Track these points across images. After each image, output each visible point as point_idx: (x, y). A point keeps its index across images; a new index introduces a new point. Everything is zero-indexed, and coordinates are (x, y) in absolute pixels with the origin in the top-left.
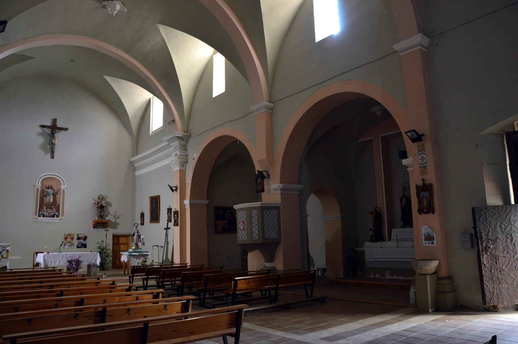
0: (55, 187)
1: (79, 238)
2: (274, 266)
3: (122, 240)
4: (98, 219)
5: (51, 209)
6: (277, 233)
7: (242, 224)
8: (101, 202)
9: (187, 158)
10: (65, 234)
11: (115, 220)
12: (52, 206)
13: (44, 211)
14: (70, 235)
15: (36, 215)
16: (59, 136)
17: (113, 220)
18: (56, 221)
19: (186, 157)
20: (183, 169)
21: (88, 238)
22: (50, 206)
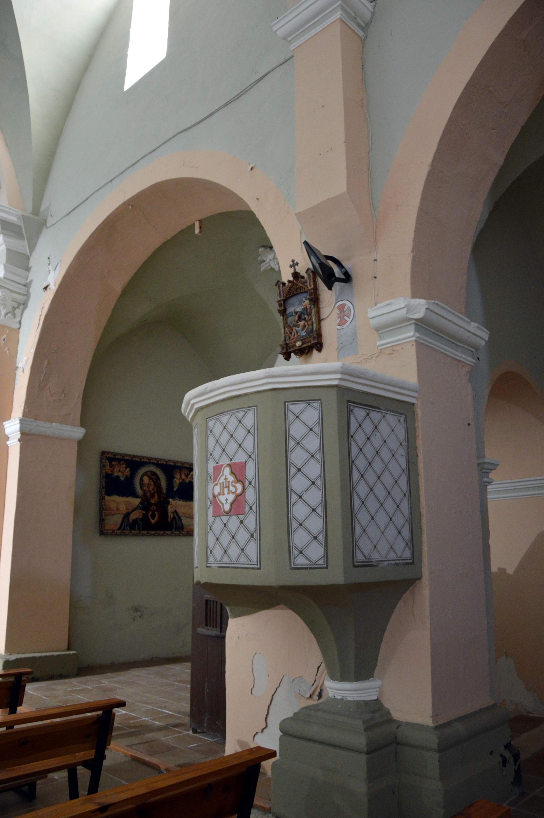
2: (375, 698)
6: (406, 533)
7: (231, 478)
9: (28, 291)
19: (23, 287)
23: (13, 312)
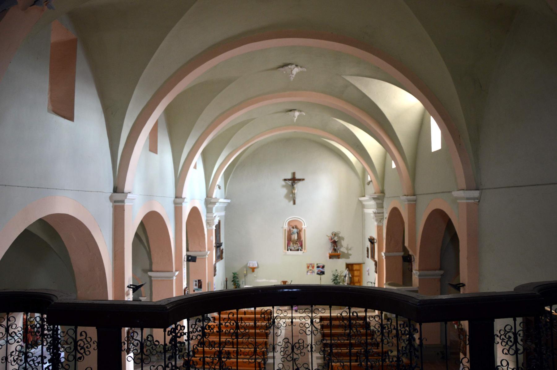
0: (299, 227)
1: (318, 267)
3: (355, 267)
4: (332, 252)
5: (296, 244)
8: (334, 238)
10: (307, 264)
11: (348, 251)
12: (297, 242)
13: (291, 246)
14: (311, 264)
15: (285, 249)
16: (299, 186)
17: (346, 251)
18: (300, 254)
20: (381, 224)
21: (325, 267)
22: (295, 242)
23: (380, 221)
